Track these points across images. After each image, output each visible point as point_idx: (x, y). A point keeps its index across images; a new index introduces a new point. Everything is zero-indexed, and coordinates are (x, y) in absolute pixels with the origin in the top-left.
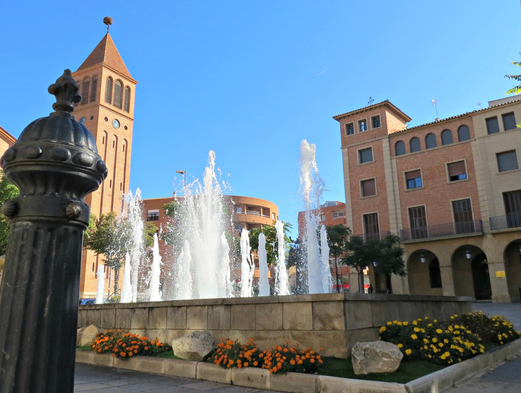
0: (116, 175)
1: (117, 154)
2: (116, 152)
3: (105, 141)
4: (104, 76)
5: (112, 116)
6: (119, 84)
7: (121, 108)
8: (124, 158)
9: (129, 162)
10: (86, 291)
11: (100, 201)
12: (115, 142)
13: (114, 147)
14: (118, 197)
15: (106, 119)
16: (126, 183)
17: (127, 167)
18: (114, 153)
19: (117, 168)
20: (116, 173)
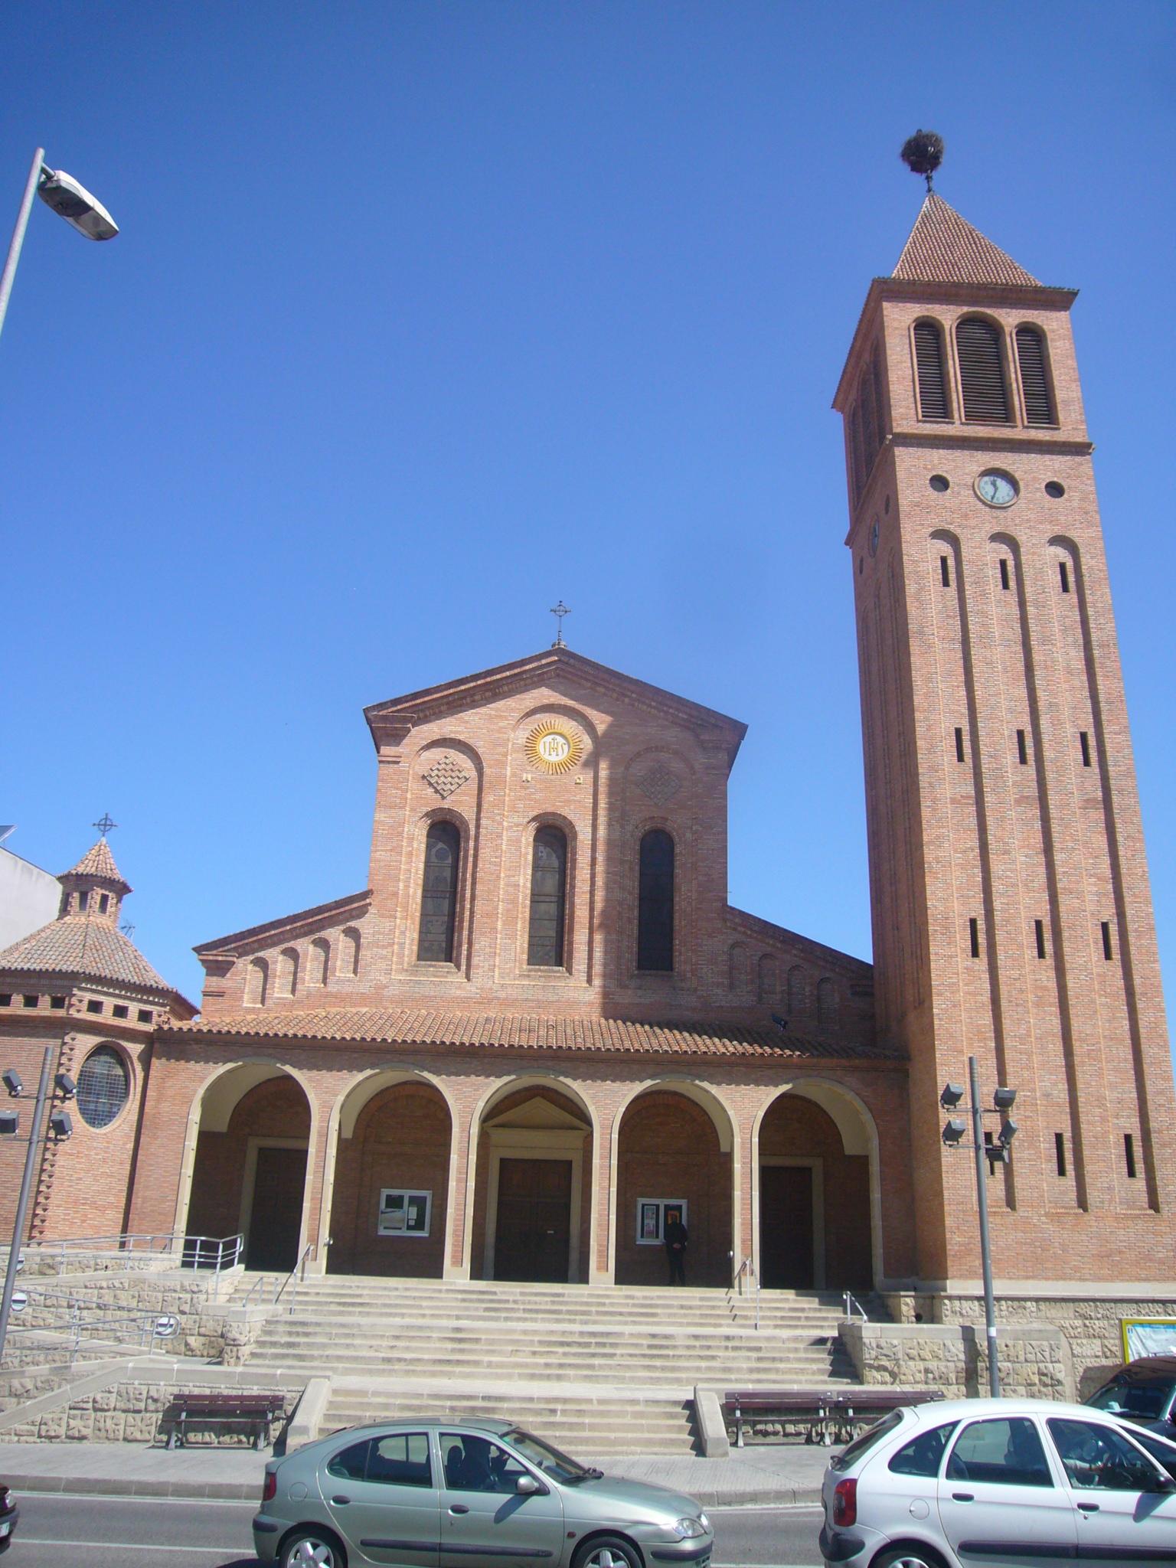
0: (1042, 705)
1: (1031, 610)
2: (1022, 604)
3: (950, 573)
4: (896, 324)
5: (963, 466)
6: (979, 333)
7: (1008, 418)
8: (1078, 618)
9: (1103, 629)
10: (962, 1277)
11: (975, 835)
12: (1011, 564)
13: (1006, 586)
14: (1076, 800)
15: (940, 483)
16: (1107, 729)
17: (1096, 653)
18: (1015, 611)
19: (1038, 673)
20: (1040, 693)
